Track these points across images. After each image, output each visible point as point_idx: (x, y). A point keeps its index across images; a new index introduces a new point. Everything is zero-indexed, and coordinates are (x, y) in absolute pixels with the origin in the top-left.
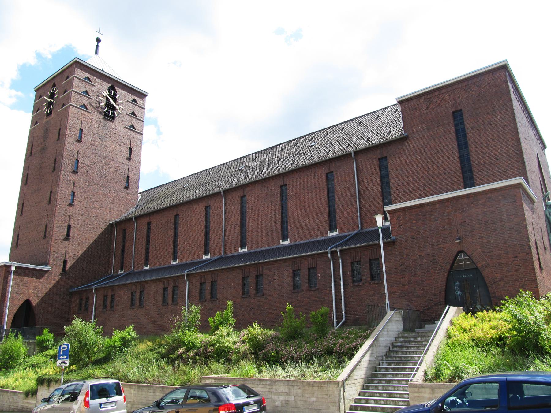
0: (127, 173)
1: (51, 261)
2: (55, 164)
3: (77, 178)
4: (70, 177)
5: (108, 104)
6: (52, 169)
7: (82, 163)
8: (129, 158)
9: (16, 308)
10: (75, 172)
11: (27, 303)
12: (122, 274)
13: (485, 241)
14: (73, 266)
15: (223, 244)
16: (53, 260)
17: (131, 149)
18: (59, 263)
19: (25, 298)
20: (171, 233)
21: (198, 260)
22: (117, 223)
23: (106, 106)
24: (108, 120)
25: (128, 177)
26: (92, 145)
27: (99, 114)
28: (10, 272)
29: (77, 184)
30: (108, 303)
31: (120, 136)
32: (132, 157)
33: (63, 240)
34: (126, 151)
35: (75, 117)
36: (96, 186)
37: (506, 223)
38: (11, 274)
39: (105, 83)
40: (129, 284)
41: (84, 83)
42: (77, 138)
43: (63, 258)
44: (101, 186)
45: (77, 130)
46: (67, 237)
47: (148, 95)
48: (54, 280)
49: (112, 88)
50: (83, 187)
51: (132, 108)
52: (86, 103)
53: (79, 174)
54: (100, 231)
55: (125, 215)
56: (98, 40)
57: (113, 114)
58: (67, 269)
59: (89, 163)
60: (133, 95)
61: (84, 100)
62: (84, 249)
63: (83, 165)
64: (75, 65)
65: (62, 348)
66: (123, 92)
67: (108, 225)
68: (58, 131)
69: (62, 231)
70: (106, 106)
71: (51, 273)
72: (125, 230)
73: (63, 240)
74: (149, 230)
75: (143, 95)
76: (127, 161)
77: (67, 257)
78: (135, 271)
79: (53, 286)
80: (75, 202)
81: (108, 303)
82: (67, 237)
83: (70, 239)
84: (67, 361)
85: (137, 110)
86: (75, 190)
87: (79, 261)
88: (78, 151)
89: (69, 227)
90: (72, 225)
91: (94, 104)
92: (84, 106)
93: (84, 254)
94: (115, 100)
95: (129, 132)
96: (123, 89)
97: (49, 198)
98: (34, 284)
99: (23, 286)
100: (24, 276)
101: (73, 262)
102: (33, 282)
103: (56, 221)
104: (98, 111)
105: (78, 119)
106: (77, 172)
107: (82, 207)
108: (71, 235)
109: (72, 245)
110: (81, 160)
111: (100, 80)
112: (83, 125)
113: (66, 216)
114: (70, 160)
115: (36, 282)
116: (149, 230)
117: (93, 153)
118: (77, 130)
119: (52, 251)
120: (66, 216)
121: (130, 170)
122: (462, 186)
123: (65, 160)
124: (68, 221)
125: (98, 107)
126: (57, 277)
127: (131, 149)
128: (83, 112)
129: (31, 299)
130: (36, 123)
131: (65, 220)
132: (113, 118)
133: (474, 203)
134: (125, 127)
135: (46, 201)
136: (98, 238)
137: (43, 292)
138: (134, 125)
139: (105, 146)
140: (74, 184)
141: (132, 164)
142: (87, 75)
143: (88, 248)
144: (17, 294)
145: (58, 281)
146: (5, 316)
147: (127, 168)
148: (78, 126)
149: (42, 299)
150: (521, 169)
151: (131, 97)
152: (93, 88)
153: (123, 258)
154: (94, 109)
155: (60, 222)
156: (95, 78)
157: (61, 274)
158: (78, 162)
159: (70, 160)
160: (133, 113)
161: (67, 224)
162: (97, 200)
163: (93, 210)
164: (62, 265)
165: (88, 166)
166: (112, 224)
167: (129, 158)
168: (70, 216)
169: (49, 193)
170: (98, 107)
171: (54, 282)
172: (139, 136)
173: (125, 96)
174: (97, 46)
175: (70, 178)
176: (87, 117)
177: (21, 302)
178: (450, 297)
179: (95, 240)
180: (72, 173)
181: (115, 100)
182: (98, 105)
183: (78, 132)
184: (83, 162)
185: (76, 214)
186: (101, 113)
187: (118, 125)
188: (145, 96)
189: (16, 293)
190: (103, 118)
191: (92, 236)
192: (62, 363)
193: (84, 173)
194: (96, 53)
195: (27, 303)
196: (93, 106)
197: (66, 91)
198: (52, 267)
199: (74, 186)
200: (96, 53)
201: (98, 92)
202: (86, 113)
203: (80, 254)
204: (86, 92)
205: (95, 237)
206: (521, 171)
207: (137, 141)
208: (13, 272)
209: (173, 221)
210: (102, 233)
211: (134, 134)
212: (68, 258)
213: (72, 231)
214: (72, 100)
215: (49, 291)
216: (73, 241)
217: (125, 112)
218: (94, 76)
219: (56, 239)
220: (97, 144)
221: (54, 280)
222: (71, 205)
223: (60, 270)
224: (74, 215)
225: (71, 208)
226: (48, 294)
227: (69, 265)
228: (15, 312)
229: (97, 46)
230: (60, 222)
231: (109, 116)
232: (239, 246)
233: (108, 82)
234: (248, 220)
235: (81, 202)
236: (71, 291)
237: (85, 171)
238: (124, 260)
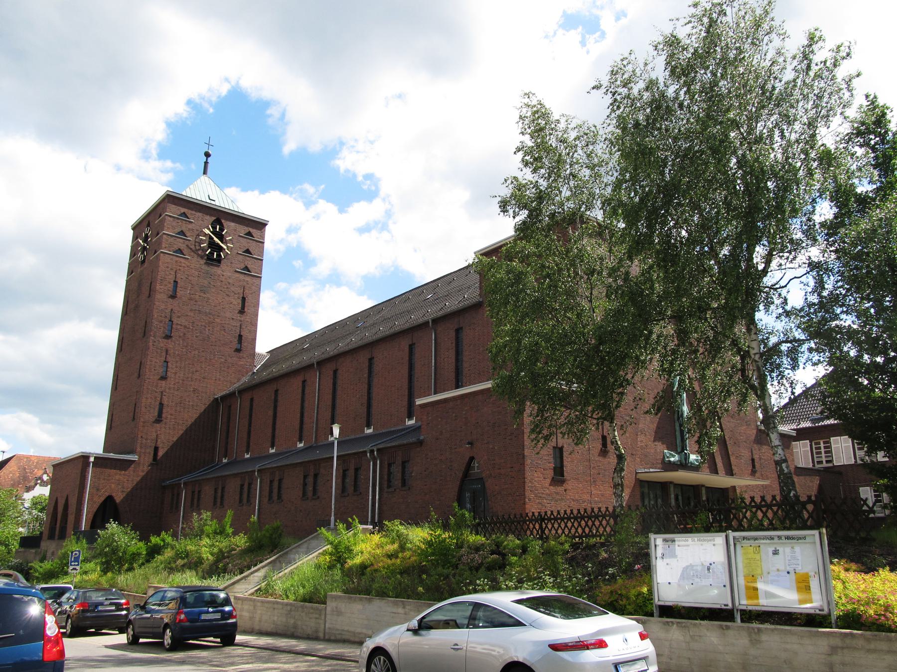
0: (238, 331)
1: (138, 449)
3: (170, 344)
4: (163, 343)
5: (212, 245)
6: (142, 334)
7: (177, 324)
8: (242, 311)
9: (96, 506)
10: (168, 337)
11: (110, 499)
14: (166, 454)
16: (141, 448)
17: (244, 299)
18: (148, 451)
19: (107, 494)
20: (271, 413)
22: (224, 398)
23: (209, 247)
24: (212, 265)
25: (240, 336)
26: (191, 299)
27: (199, 259)
28: (88, 464)
29: (171, 352)
30: (219, 500)
31: (229, 283)
32: (246, 310)
33: (154, 422)
34: (237, 303)
35: (168, 267)
36: (196, 352)
38: (89, 466)
39: (208, 217)
40: (213, 478)
41: (179, 221)
42: (171, 293)
43: (154, 445)
44: (203, 351)
45: (170, 283)
46: (159, 419)
47: (269, 223)
48: (143, 471)
49: (218, 221)
50: (178, 355)
51: (245, 243)
52: (183, 247)
54: (202, 408)
55: (236, 385)
56: (207, 155)
57: (219, 255)
58: (158, 458)
59: (186, 324)
60: (247, 226)
61: (180, 244)
62: (181, 432)
63: (179, 327)
64: (166, 200)
66: (232, 224)
67: (213, 401)
68: (149, 285)
69: (152, 411)
70: (209, 247)
71: (139, 464)
72: (230, 407)
73: (154, 422)
74: (251, 405)
75: (261, 225)
76: (239, 315)
77: (158, 443)
78: (238, 459)
79: (142, 479)
80: (169, 374)
81: (219, 500)
82: (159, 419)
83: (162, 421)
85: (252, 247)
86: (169, 359)
87: (175, 446)
88: (172, 310)
89: (161, 405)
90: (165, 402)
91: (193, 247)
92: (180, 251)
93: (181, 438)
94: (221, 238)
95: (242, 277)
96: (233, 221)
98: (117, 477)
99: (104, 479)
100: (106, 467)
101: (166, 449)
102: (117, 475)
103: (144, 400)
104: (198, 255)
105: (172, 269)
106: (171, 337)
107: (177, 381)
108: (164, 415)
109: (165, 428)
110: (175, 320)
111: (200, 214)
112: (178, 275)
113: (156, 392)
114: (161, 322)
115: (120, 474)
116: (251, 405)
117: (191, 310)
118: (170, 283)
119: (139, 436)
120: (156, 392)
121: (243, 327)
123: (155, 323)
124: (159, 399)
125: (199, 250)
126: (146, 469)
127: (244, 299)
128: (177, 259)
129: (114, 495)
130: (132, 273)
131: (156, 398)
132: (219, 260)
134: (236, 271)
135: (136, 375)
136: (199, 417)
137: (129, 486)
138: (249, 266)
139: (209, 299)
140: (167, 351)
141: (246, 318)
142: (183, 210)
143: (186, 431)
144: (98, 490)
145: (147, 473)
146: (83, 515)
147: (238, 325)
148: (171, 278)
149: (127, 495)
151: (243, 230)
152: (190, 226)
153: (227, 443)
154: (192, 253)
155: (149, 400)
156: (194, 212)
157: (151, 465)
158: (172, 324)
159: (161, 322)
160: (248, 251)
161: (158, 403)
162: (199, 369)
163: (193, 383)
164: (152, 453)
165: (185, 327)
166: (217, 399)
167: (242, 311)
168: (162, 392)
169: (139, 364)
170: (199, 250)
171: (142, 474)
172: (255, 280)
173: (235, 230)
174: (206, 163)
175: (162, 345)
176: (183, 265)
177: (102, 499)
179: (196, 421)
180: (164, 338)
181: (221, 238)
182: (198, 248)
183: (171, 286)
184: (179, 323)
185: (170, 388)
186: (202, 257)
187: (225, 271)
188: (266, 225)
189: (96, 488)
190: (205, 263)
191: (190, 416)
193: (180, 337)
194: (205, 173)
195: (110, 499)
196: (191, 249)
197: (158, 234)
198: (140, 457)
199: (167, 354)
200: (205, 173)
201: (197, 230)
202: (182, 260)
203: (175, 439)
204: (182, 233)
205: (196, 416)
207: (253, 287)
209: (273, 398)
210: (205, 410)
211: (248, 279)
212: (160, 445)
213: (164, 411)
214: (163, 246)
215: (137, 484)
216: (166, 423)
217: (236, 251)
218: (192, 210)
219: (144, 422)
220: (197, 297)
221: (143, 471)
222: (164, 378)
223: (149, 459)
224: (167, 390)
225: (164, 382)
226: (135, 488)
227: (161, 453)
228: (95, 510)
229: (206, 163)
230: (149, 400)
231: (214, 260)
233: (211, 215)
235: (176, 373)
236: (163, 484)
237: (182, 334)
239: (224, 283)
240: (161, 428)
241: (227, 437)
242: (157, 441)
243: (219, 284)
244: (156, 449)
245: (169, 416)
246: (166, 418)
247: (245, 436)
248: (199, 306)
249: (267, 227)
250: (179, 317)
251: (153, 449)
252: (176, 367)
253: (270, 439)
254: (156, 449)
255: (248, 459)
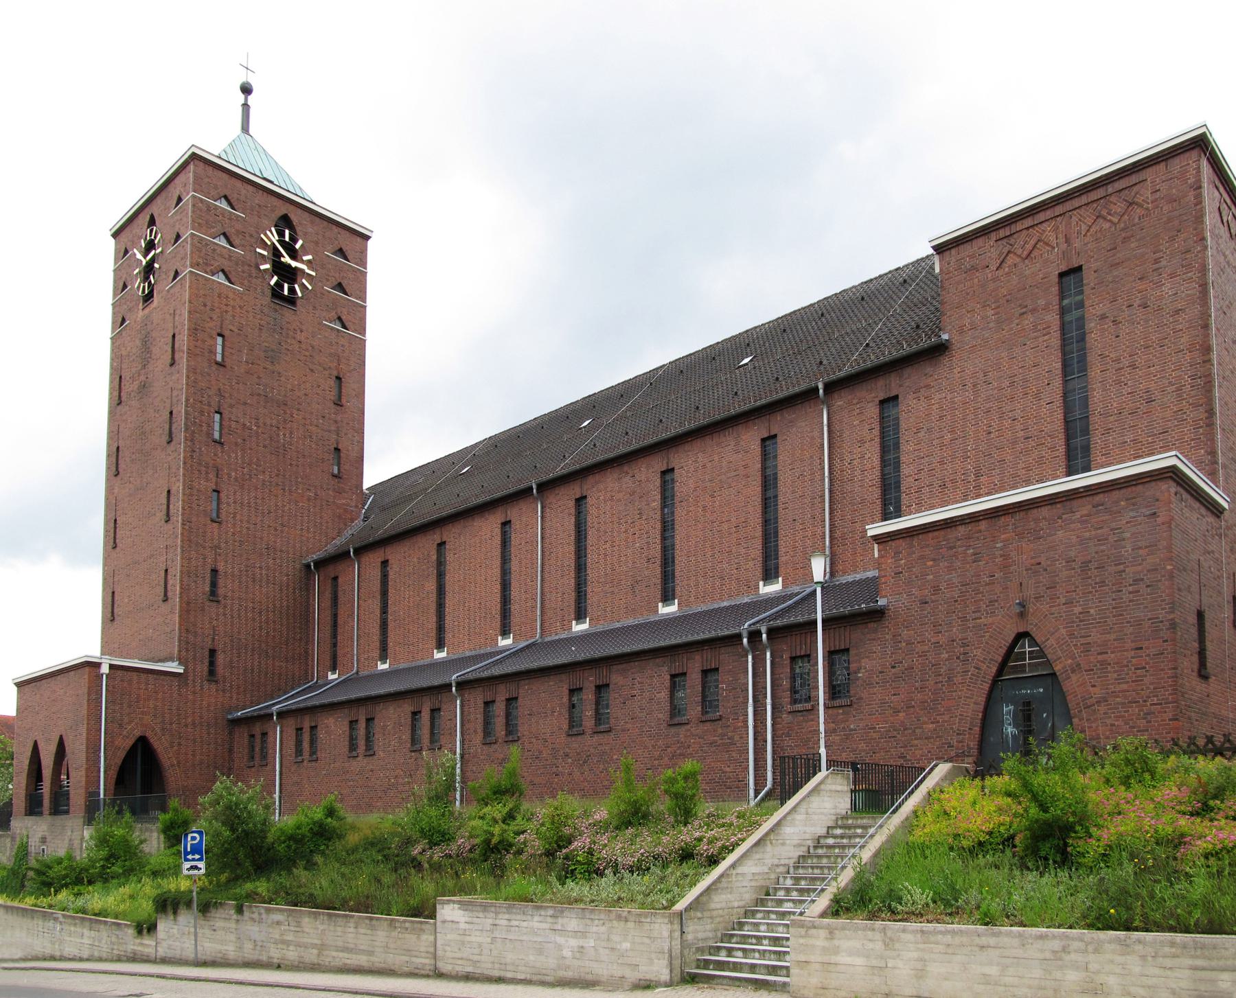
2: (171, 424)
6: (165, 438)
12: (336, 679)
13: (1077, 610)
15: (538, 614)
21: (489, 649)
37: (1128, 566)
50: (236, 479)
53: (226, 447)
63: (234, 425)
65: (189, 839)
78: (363, 673)
84: (202, 865)
97: (165, 506)
110: (226, 415)
122: (1063, 469)
133: (1064, 516)
135: (161, 515)
150: (1201, 427)
169: (165, 493)
178: (992, 739)
192: (192, 868)
193: (236, 444)
206: (1201, 430)
208: (104, 676)
232: (573, 616)
234: (591, 558)
238: (338, 648)
239: (303, 346)
240: (218, 615)
241: (334, 635)
242: (214, 639)
243: (296, 346)
244: (212, 652)
245: (229, 594)
246: (225, 597)
247: (375, 630)
248: (266, 386)
249: (370, 243)
250: (231, 406)
251: (207, 653)
252: (235, 502)
253: (433, 634)
254: (212, 652)
255: (384, 674)
